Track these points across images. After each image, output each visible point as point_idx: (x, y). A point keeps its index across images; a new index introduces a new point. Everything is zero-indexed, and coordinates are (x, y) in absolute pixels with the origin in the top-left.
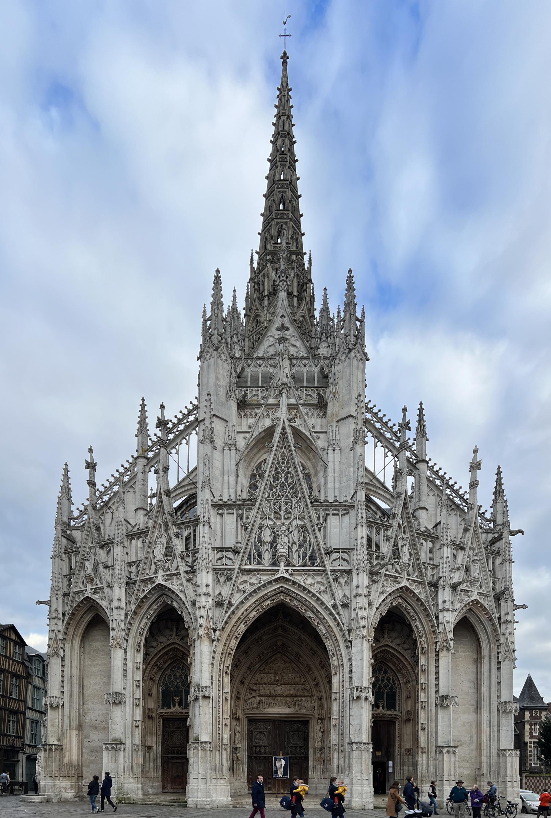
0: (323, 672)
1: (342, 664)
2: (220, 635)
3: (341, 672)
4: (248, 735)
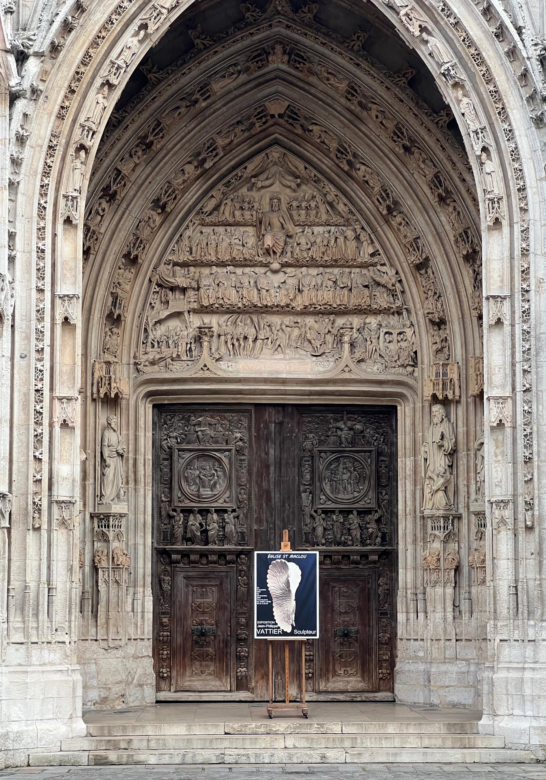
0: (444, 219)
1: (522, 189)
2: (44, 76)
3: (517, 215)
4: (156, 464)
